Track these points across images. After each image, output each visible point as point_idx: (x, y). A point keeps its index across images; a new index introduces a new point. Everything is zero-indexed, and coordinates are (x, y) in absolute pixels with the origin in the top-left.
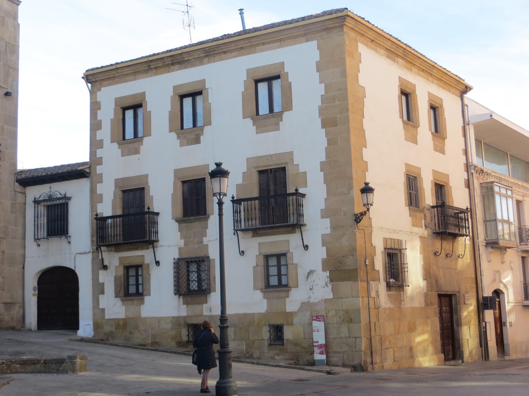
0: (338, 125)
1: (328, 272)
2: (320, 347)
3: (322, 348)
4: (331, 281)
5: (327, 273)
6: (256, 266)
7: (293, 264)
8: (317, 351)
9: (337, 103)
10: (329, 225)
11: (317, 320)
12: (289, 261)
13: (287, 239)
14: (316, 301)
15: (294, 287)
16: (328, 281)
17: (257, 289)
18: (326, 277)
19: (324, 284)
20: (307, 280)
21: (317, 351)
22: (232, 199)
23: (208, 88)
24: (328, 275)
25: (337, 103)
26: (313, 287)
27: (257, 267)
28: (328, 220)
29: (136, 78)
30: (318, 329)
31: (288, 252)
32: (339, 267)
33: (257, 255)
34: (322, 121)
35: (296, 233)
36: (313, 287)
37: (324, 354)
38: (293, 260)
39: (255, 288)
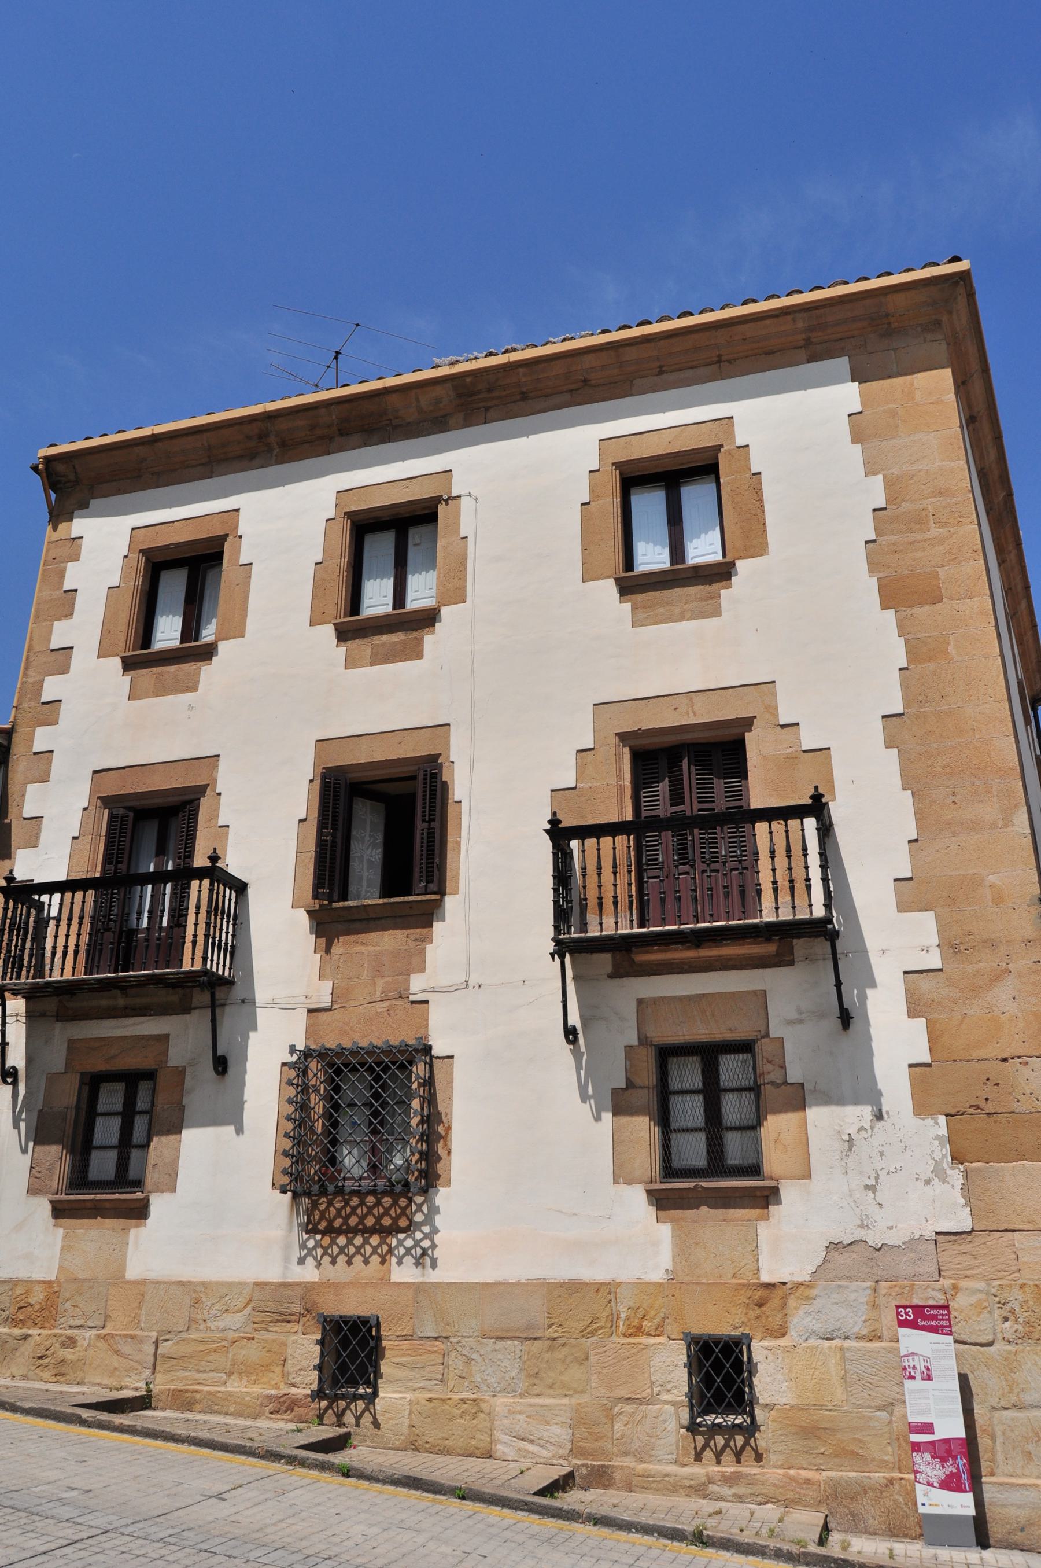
0: (945, 600)
1: (942, 1119)
2: (941, 1451)
3: (955, 1458)
4: (957, 1158)
5: (937, 1123)
6: (624, 1086)
7: (785, 1083)
8: (929, 1471)
9: (934, 531)
10: (933, 938)
11: (921, 1323)
12: (769, 1073)
13: (758, 987)
14: (894, 1239)
15: (791, 1178)
16: (944, 1156)
17: (629, 1182)
18: (937, 1143)
19: (926, 1170)
20: (850, 1150)
21: (929, 1471)
22: (548, 826)
23: (459, 497)
24: (943, 1131)
25: (934, 531)
26: (877, 1178)
27: (630, 1091)
28: (927, 920)
29: (212, 472)
30: (928, 1369)
31: (763, 1037)
32: (987, 1099)
33: (632, 1046)
34: (881, 587)
35: (796, 964)
36: (877, 1178)
37: (965, 1491)
38: (783, 1067)
39: (621, 1175)
